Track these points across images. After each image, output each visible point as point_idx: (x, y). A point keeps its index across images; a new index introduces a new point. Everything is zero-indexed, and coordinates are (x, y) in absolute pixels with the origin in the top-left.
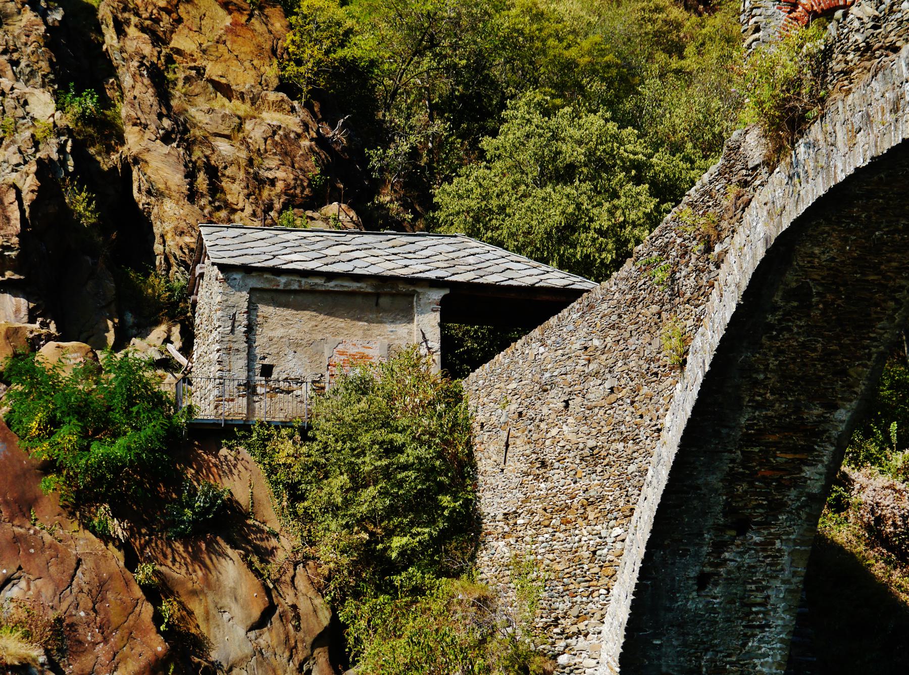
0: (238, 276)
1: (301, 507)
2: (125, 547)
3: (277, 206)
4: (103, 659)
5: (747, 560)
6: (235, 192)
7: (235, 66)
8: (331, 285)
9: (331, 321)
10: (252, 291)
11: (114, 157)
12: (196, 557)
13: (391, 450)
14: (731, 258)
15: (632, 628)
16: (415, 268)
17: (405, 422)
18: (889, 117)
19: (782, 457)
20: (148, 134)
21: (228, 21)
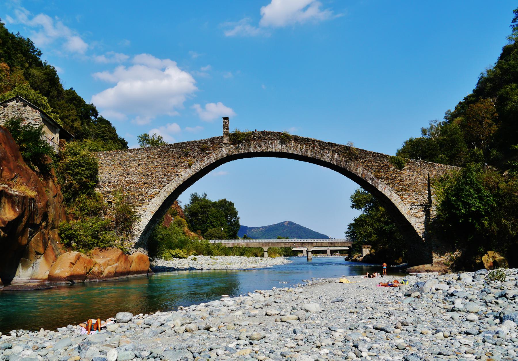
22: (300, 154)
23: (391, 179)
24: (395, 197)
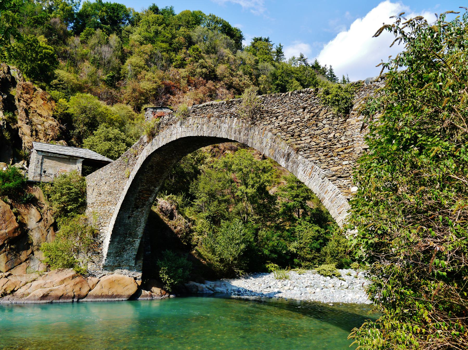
0: (40, 153)
1: (50, 199)
2: (11, 205)
3: (50, 139)
4: (4, 227)
5: (138, 214)
6: (41, 136)
7: (43, 111)
8: (60, 156)
9: (59, 163)
10: (43, 156)
11: (15, 126)
12: (26, 208)
13: (70, 189)
14: (139, 158)
15: (115, 225)
16: (78, 155)
17: (73, 184)
18: (170, 137)
19: (146, 196)
20: (23, 122)
21: (43, 102)
22: (196, 135)
23: (325, 148)
24: (331, 193)
